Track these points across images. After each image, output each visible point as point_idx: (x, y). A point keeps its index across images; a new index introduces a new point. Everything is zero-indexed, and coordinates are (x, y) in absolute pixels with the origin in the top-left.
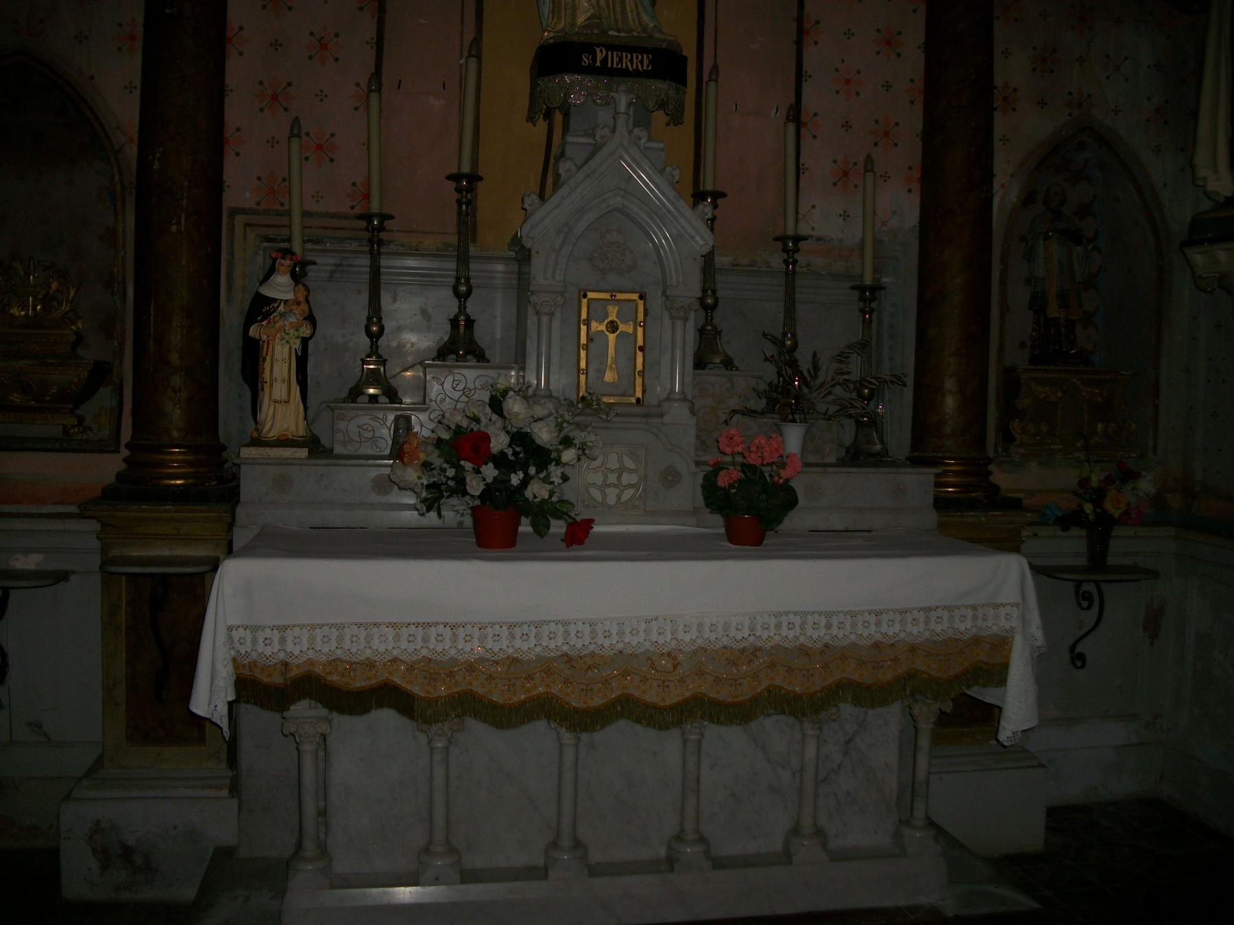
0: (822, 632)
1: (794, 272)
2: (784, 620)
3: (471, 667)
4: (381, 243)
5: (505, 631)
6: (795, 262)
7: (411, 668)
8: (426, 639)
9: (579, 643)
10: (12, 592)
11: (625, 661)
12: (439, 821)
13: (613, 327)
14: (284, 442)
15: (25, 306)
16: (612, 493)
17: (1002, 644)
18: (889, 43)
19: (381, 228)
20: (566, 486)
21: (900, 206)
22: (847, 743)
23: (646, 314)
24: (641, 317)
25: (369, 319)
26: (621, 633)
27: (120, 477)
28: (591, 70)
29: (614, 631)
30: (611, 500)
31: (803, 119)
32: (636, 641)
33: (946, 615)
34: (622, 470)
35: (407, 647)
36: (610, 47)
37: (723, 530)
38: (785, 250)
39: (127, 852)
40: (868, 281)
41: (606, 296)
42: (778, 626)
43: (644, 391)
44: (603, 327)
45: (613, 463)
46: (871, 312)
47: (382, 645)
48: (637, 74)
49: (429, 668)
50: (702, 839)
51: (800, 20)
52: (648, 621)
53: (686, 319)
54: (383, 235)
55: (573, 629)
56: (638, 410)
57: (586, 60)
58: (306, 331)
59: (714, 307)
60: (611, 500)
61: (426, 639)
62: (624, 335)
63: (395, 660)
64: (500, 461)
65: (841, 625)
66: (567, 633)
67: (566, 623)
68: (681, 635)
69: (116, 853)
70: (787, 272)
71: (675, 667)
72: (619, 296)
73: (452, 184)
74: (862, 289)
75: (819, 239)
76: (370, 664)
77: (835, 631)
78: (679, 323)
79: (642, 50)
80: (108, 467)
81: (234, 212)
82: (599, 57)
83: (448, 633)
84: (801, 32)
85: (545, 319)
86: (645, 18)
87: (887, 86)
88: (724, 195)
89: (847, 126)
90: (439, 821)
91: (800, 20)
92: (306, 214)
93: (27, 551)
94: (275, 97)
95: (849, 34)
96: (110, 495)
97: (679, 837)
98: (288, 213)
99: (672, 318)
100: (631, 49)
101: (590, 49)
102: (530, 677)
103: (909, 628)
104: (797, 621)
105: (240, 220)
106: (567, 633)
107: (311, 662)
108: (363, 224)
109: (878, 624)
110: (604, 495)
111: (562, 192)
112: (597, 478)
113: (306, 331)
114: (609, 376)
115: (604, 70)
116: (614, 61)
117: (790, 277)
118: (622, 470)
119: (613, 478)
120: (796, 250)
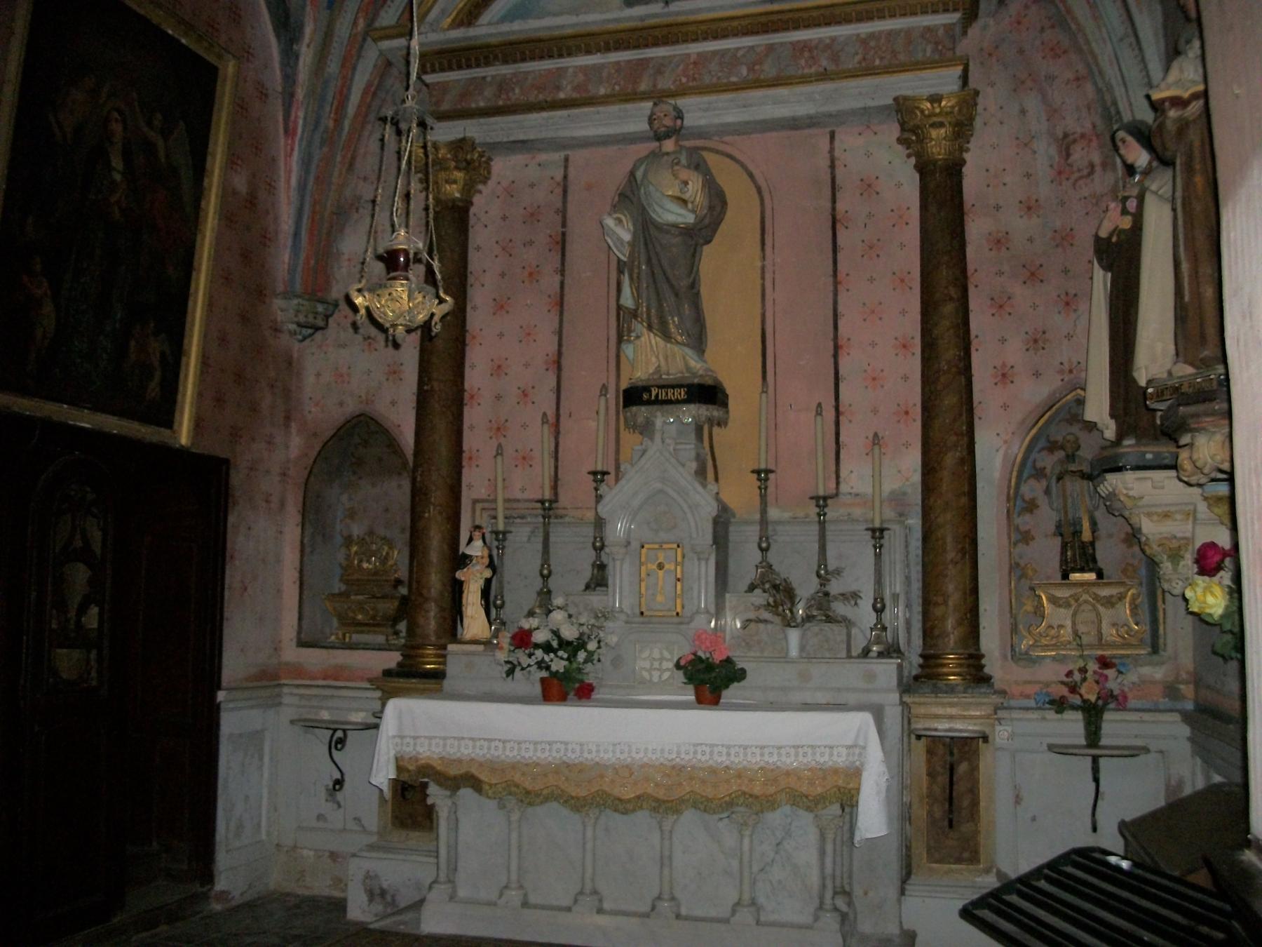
0: (724, 758)
1: (825, 521)
2: (699, 749)
3: (514, 766)
4: (549, 517)
5: (532, 747)
6: (825, 515)
7: (481, 765)
8: (489, 748)
9: (572, 757)
10: (349, 733)
11: (599, 769)
12: (514, 866)
13: (661, 566)
14: (474, 642)
15: (369, 561)
16: (656, 674)
17: (856, 773)
18: (904, 346)
19: (550, 509)
20: (589, 667)
21: (907, 467)
22: (778, 844)
23: (683, 557)
24: (679, 559)
25: (542, 566)
26: (598, 751)
27: (399, 665)
28: (649, 403)
29: (594, 749)
30: (656, 679)
31: (841, 409)
32: (608, 757)
33: (810, 751)
34: (662, 659)
35: (480, 752)
36: (661, 387)
37: (693, 698)
38: (818, 506)
39: (383, 893)
40: (877, 525)
41: (656, 546)
42: (695, 752)
43: (683, 607)
44: (655, 567)
45: (656, 654)
46: (880, 547)
47: (466, 751)
48: (678, 402)
49: (494, 766)
50: (673, 899)
51: (836, 338)
52: (614, 745)
53: (707, 560)
54: (551, 512)
55: (570, 747)
56: (676, 620)
57: (645, 396)
58: (488, 574)
59: (767, 549)
60: (656, 679)
61: (489, 748)
62: (669, 571)
63: (472, 760)
64: (547, 648)
65: (737, 755)
66: (566, 749)
67: (566, 744)
68: (634, 755)
69: (377, 893)
70: (819, 522)
71: (631, 774)
72: (665, 546)
73: (591, 477)
74: (873, 530)
75: (857, 495)
76: (460, 761)
77: (732, 758)
78: (703, 563)
79: (680, 386)
80: (392, 659)
81: (475, 502)
82: (654, 393)
83: (500, 745)
84: (837, 348)
85: (618, 563)
86: (692, 363)
87: (905, 378)
88: (772, 471)
89: (875, 411)
90: (514, 866)
91: (836, 338)
92: (507, 501)
93: (358, 710)
94: (498, 429)
95: (873, 344)
96: (388, 673)
97: (659, 898)
98: (495, 501)
99: (699, 559)
100: (673, 387)
101: (647, 389)
102: (545, 775)
103: (784, 759)
104: (708, 750)
105: (479, 506)
106: (566, 749)
107: (429, 758)
108: (539, 505)
109: (762, 755)
110: (651, 676)
111: (623, 482)
112: (647, 665)
113: (488, 574)
114: (660, 598)
115: (657, 402)
116: (662, 396)
117: (822, 524)
118: (662, 659)
119: (656, 665)
120: (826, 506)
